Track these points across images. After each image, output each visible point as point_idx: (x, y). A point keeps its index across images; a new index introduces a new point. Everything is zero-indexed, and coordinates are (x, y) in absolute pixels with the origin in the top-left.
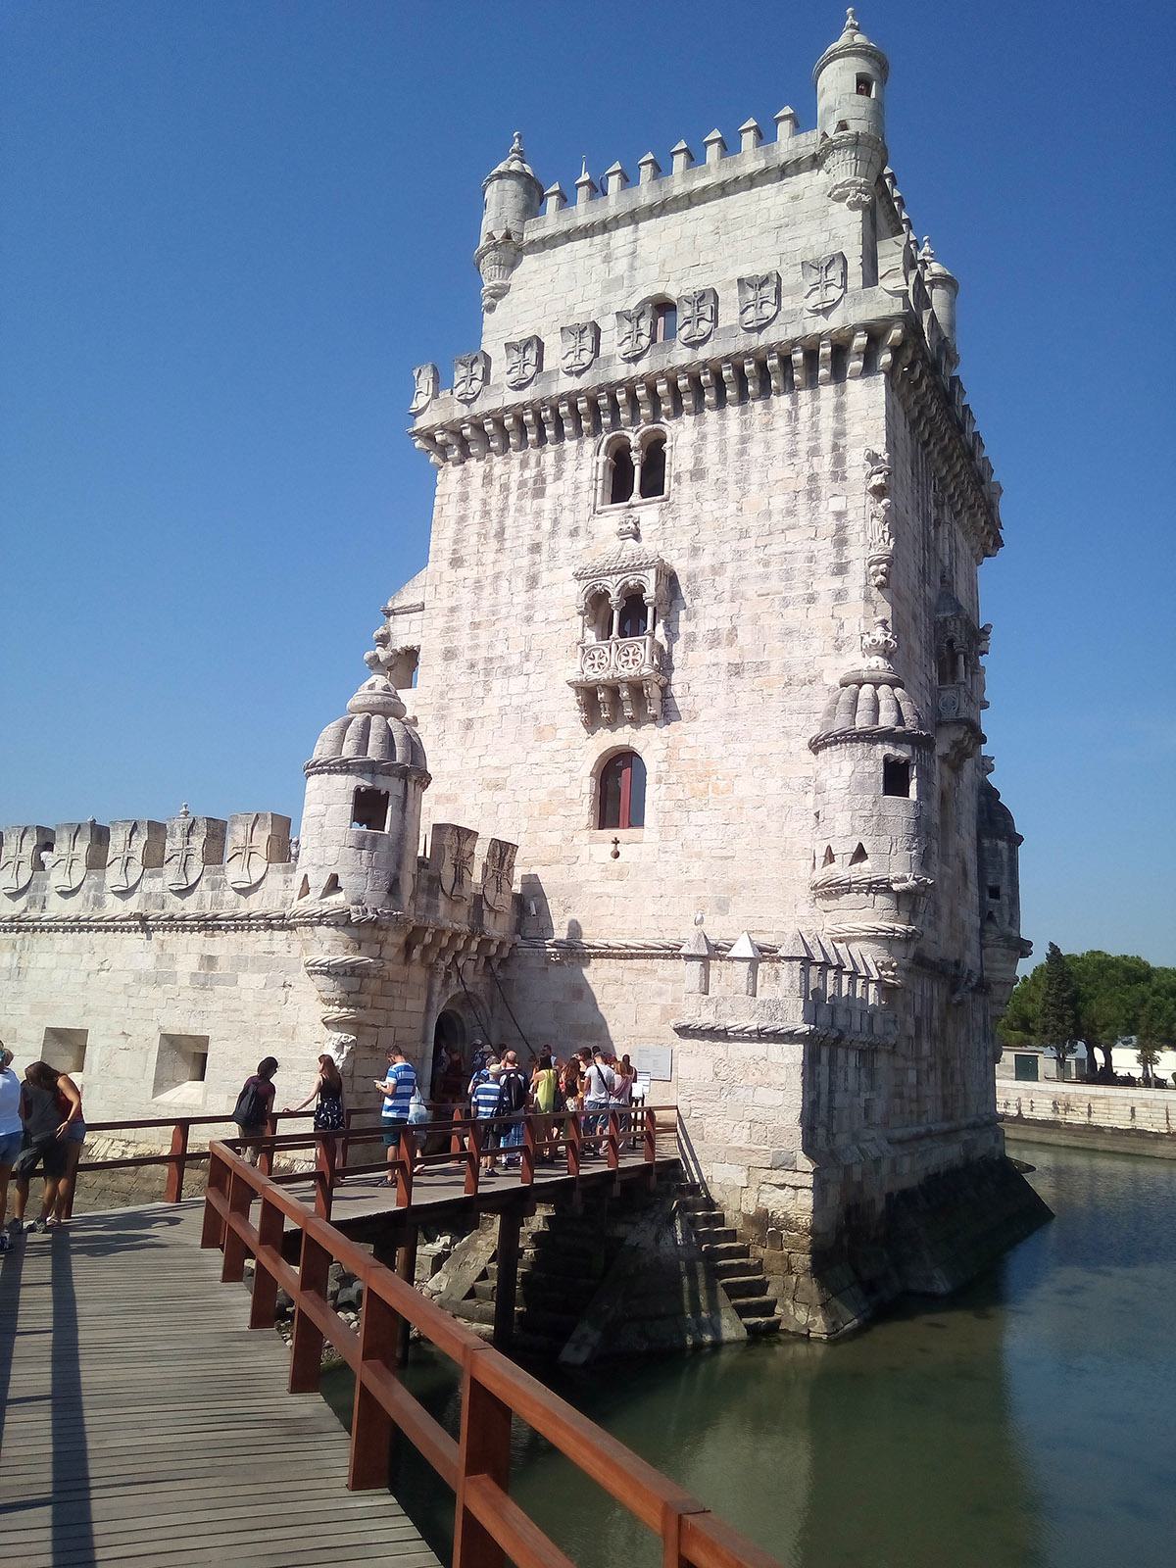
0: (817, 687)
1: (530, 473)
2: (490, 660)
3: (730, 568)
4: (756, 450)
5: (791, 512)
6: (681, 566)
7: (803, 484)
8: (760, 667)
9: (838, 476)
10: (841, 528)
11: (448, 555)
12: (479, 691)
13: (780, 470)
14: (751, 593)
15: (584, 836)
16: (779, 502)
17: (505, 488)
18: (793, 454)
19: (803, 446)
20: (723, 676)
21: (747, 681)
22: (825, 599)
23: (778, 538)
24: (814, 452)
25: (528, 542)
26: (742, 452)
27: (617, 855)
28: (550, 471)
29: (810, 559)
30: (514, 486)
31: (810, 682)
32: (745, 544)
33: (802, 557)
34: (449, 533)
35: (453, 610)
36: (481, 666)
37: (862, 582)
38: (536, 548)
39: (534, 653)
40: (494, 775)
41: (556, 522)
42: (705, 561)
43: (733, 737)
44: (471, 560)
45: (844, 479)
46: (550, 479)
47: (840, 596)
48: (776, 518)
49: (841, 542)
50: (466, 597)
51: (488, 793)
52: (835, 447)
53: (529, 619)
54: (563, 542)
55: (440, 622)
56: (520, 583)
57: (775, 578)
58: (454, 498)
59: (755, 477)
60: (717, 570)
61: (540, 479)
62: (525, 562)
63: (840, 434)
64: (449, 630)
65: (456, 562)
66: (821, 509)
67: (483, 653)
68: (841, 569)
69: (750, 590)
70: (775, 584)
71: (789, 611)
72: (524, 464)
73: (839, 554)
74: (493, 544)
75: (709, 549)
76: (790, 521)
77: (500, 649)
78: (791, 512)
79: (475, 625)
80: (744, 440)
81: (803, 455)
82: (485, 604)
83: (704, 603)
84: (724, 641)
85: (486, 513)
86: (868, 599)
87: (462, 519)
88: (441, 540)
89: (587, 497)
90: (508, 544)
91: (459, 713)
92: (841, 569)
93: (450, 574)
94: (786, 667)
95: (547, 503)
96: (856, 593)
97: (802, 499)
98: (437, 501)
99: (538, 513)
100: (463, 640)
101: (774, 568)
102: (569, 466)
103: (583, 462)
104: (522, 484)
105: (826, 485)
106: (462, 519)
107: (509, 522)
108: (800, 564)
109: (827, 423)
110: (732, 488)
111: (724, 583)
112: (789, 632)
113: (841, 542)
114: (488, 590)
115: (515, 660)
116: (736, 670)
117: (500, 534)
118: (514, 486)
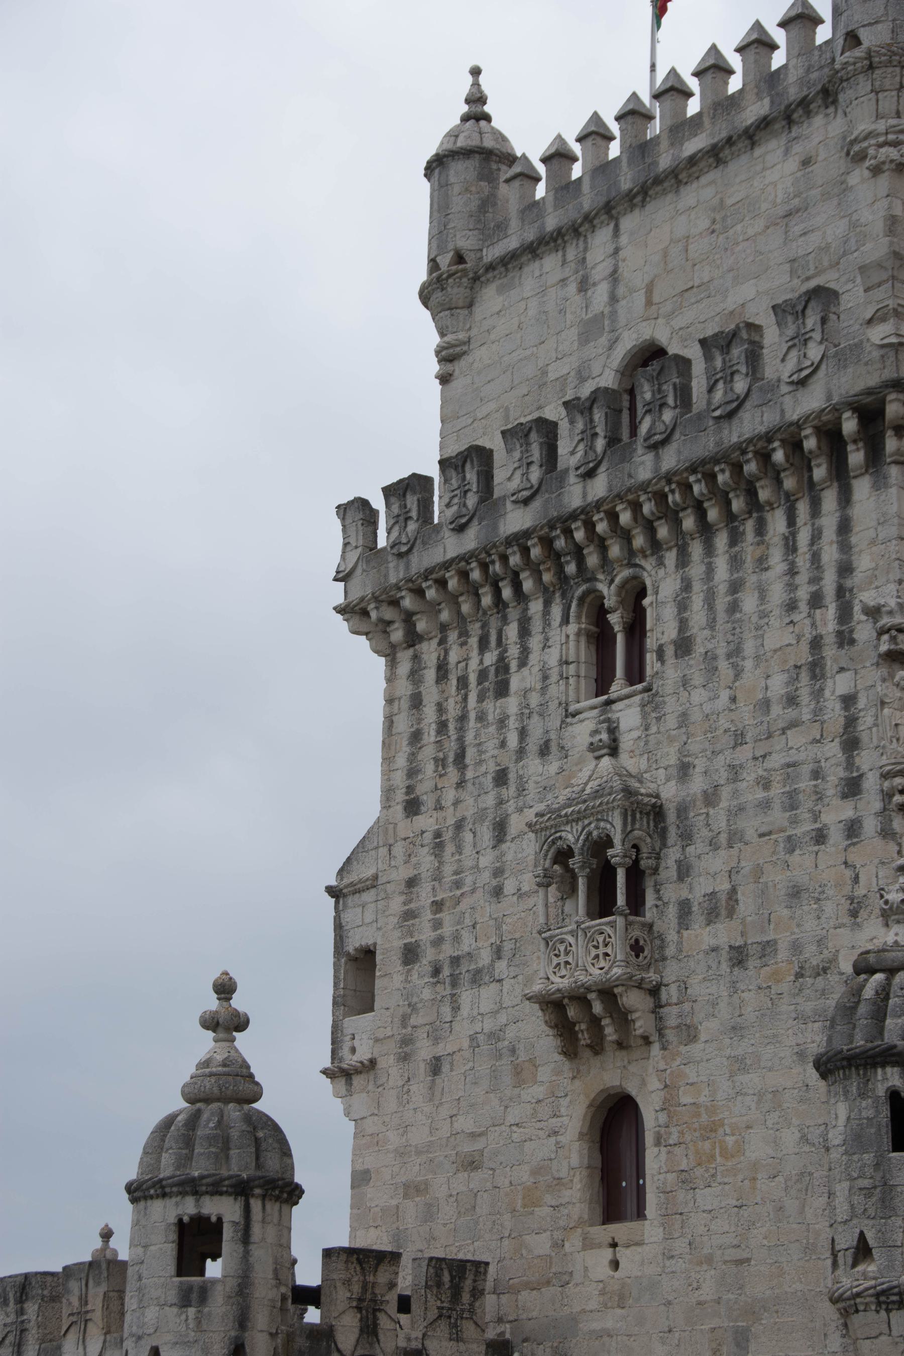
0: (833, 978)
1: (490, 658)
2: (455, 961)
3: (725, 792)
4: (749, 603)
7: (804, 655)
8: (768, 948)
9: (845, 639)
10: (851, 722)
12: (446, 1010)
13: (777, 635)
16: (778, 685)
17: (463, 682)
18: (791, 606)
19: (803, 594)
20: (725, 967)
22: (836, 836)
23: (778, 743)
24: (816, 601)
25: (492, 767)
26: (734, 608)
28: (514, 651)
29: (816, 774)
30: (473, 678)
31: (825, 970)
32: (744, 754)
33: (806, 770)
35: (412, 883)
36: (446, 972)
37: (878, 805)
38: (501, 778)
39: (508, 946)
40: (467, 1147)
42: (697, 784)
43: (739, 1065)
44: (428, 801)
45: (852, 642)
46: (514, 665)
47: (853, 829)
48: (776, 710)
49: (851, 744)
50: (426, 860)
52: (841, 592)
53: (498, 892)
54: (533, 766)
56: (486, 834)
57: (777, 806)
59: (749, 647)
60: (710, 798)
61: (502, 666)
62: (490, 800)
63: (845, 569)
64: (409, 915)
66: (827, 693)
67: (448, 950)
68: (852, 788)
69: (750, 825)
70: (778, 816)
71: (795, 858)
73: (850, 764)
75: (700, 764)
77: (467, 943)
78: (792, 700)
80: (735, 587)
81: (803, 606)
83: (699, 851)
84: (723, 912)
90: (469, 774)
91: (424, 1051)
94: (796, 947)
95: (512, 704)
96: (870, 825)
99: (502, 722)
100: (425, 934)
101: (777, 790)
102: (535, 642)
104: (483, 675)
105: (830, 652)
107: (470, 737)
108: (805, 784)
109: (830, 554)
110: (723, 665)
112: (795, 893)
113: (851, 744)
114: (450, 848)
115: (485, 958)
116: (739, 957)
117: (460, 756)
118: (473, 678)
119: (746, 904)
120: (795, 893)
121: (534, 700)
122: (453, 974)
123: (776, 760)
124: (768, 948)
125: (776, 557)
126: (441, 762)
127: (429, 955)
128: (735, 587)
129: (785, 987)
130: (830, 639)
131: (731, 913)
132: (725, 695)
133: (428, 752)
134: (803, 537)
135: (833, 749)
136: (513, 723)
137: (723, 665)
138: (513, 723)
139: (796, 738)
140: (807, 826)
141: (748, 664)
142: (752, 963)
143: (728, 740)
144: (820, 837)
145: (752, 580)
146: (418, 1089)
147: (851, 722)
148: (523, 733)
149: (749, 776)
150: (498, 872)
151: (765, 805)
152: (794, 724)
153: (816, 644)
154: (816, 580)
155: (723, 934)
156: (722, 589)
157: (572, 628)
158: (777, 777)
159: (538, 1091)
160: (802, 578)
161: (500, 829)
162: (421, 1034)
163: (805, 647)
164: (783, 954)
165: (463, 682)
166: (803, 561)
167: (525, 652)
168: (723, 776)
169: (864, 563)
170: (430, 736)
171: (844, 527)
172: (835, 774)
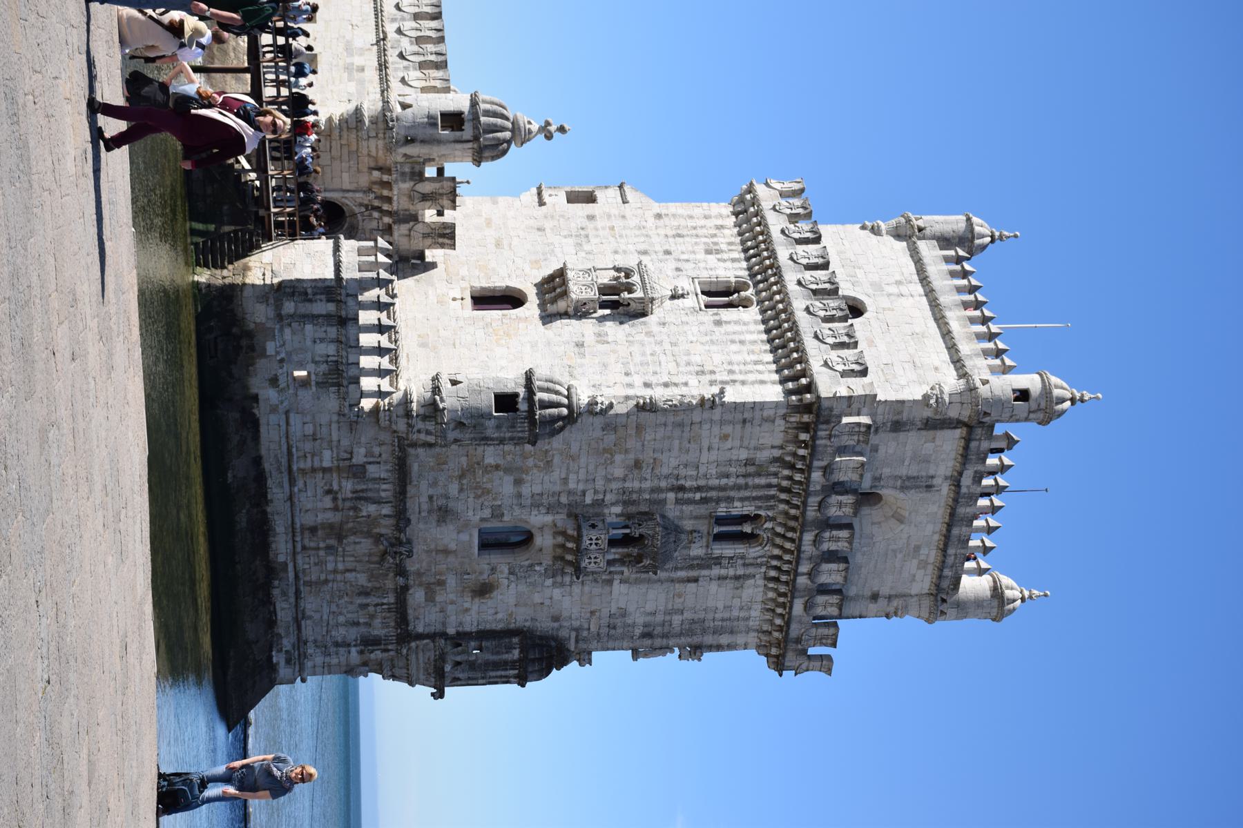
1: (724, 247)
2: (587, 236)
3: (651, 339)
4: (734, 347)
5: (688, 364)
6: (651, 319)
7: (707, 368)
8: (583, 355)
9: (712, 383)
10: (676, 385)
11: (664, 212)
12: (565, 233)
13: (718, 358)
14: (632, 349)
15: (466, 285)
16: (697, 359)
17: (715, 236)
18: (730, 363)
19: (735, 368)
21: (572, 349)
22: (628, 380)
23: (672, 358)
24: (731, 372)
25: (672, 249)
26: (733, 342)
27: (454, 299)
28: (725, 256)
30: (715, 240)
32: (667, 346)
34: (680, 211)
35: (624, 217)
36: (582, 232)
38: (668, 252)
39: (591, 257)
40: (505, 242)
41: (688, 261)
42: (655, 329)
43: (534, 345)
44: (660, 223)
46: (719, 256)
47: (630, 385)
48: (685, 358)
49: (666, 385)
50: (633, 222)
51: (493, 241)
52: (734, 381)
53: (616, 252)
54: (673, 265)
55: (614, 211)
56: (642, 247)
58: (707, 213)
59: (714, 348)
60: (649, 334)
61: (718, 252)
62: (658, 248)
63: (743, 383)
64: (609, 216)
65: (659, 216)
67: (591, 233)
68: (647, 385)
69: (635, 349)
70: (638, 359)
71: (620, 365)
72: (730, 244)
73: (658, 385)
74: (670, 233)
75: (665, 330)
76: (683, 363)
77: (593, 240)
79: (612, 228)
80: (742, 342)
81: (730, 367)
82: (628, 232)
85: (695, 228)
86: (627, 398)
87: (691, 217)
88: (673, 208)
89: (705, 275)
90: (671, 240)
91: (548, 225)
92: (647, 385)
93: (649, 215)
94: (581, 366)
95: (701, 256)
96: (631, 392)
97: (699, 369)
98: (705, 205)
99: (694, 252)
100: (599, 223)
101: (650, 358)
102: (729, 264)
103: (732, 269)
104: (716, 244)
105: (708, 377)
106: (691, 217)
107: (687, 239)
109: (751, 377)
110: (708, 338)
111: (642, 337)
112: (605, 366)
113: (666, 385)
114: (637, 232)
115: (587, 247)
117: (679, 236)
118: (715, 240)
120: (605, 366)
121: (702, 265)
122: (582, 236)
123: (663, 358)
124: (583, 355)
126: (678, 227)
127: (590, 225)
128: (742, 342)
130: (713, 377)
131: (598, 342)
132: (694, 339)
133: (683, 222)
134: (760, 367)
135: (665, 379)
136: (692, 257)
137: (708, 338)
138: (692, 257)
139: (672, 367)
140: (632, 369)
141: (707, 348)
142: (576, 349)
144: (627, 374)
145: (744, 348)
146: (532, 222)
147: (676, 385)
148: (688, 261)
149: (658, 349)
150: (625, 252)
151: (644, 354)
153: (713, 372)
154: (741, 372)
155: (589, 339)
156: (742, 338)
157: (733, 280)
158: (655, 358)
159: (527, 270)
160: (742, 367)
161: (645, 253)
162: (556, 223)
163: (711, 368)
164: (579, 361)
165: (715, 236)
166: (750, 367)
167: (725, 261)
168: (659, 339)
169: (746, 389)
170: (690, 223)
171: (762, 382)
172: (653, 380)
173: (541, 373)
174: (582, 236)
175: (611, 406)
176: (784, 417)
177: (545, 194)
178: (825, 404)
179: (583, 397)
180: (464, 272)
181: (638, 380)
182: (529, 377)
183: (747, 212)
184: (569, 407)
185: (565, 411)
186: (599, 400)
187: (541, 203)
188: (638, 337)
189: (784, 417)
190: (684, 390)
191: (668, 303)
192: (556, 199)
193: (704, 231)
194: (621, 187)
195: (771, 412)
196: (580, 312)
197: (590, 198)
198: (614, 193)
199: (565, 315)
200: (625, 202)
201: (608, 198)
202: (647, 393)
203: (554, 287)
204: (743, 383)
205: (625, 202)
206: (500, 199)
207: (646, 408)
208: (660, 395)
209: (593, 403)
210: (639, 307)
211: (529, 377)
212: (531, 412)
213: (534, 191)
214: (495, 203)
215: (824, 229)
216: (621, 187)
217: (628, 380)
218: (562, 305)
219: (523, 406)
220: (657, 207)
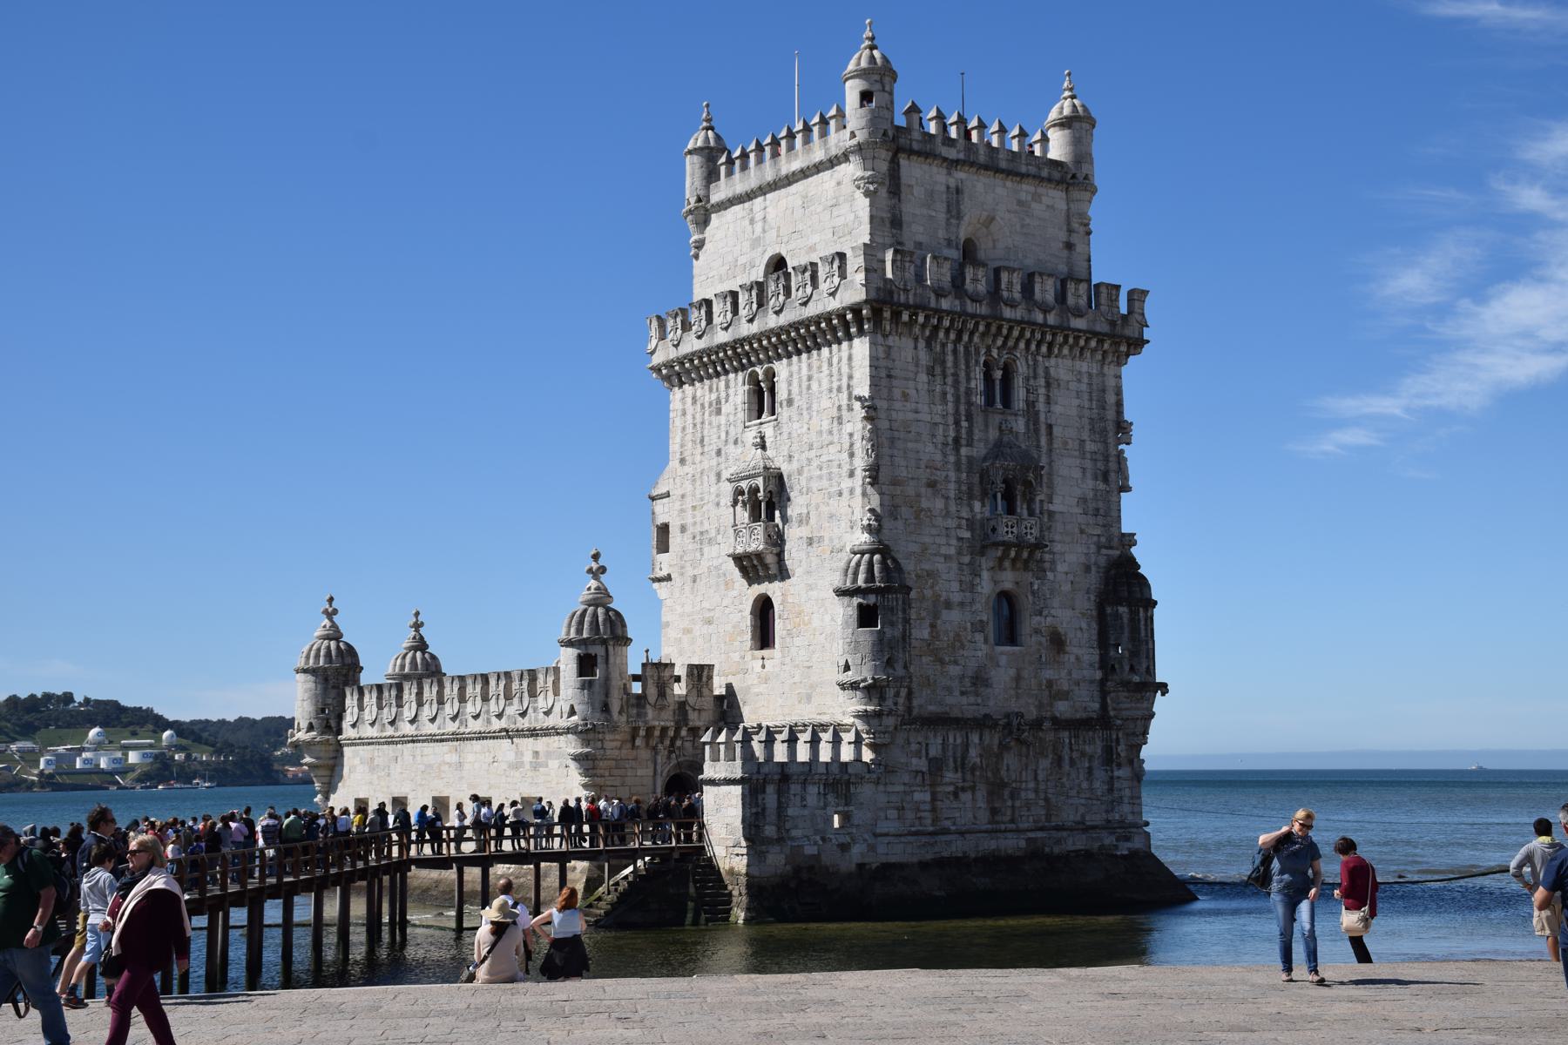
1: (714, 396)
4: (815, 386)
5: (831, 432)
7: (835, 413)
8: (821, 539)
9: (850, 409)
10: (852, 445)
13: (826, 403)
16: (826, 425)
17: (702, 405)
18: (830, 391)
19: (835, 385)
21: (815, 550)
22: (846, 494)
23: (825, 450)
24: (839, 389)
26: (809, 388)
28: (723, 395)
29: (839, 466)
32: (812, 454)
34: (678, 440)
35: (683, 496)
38: (719, 453)
42: (795, 465)
43: (810, 587)
47: (852, 491)
49: (852, 455)
50: (688, 487)
52: (849, 386)
53: (718, 504)
54: (731, 447)
55: (677, 505)
56: (713, 478)
59: (815, 407)
60: (800, 472)
61: (718, 402)
62: (714, 462)
63: (850, 377)
64: (682, 511)
65: (683, 461)
67: (699, 528)
68: (852, 474)
69: (815, 485)
70: (825, 483)
72: (711, 390)
74: (699, 450)
75: (796, 456)
77: (706, 526)
79: (694, 508)
80: (810, 378)
86: (864, 494)
87: (684, 429)
88: (674, 447)
89: (741, 415)
91: (690, 572)
92: (852, 474)
93: (681, 470)
94: (831, 540)
95: (722, 419)
96: (858, 491)
100: (689, 521)
101: (825, 471)
102: (731, 391)
103: (736, 389)
104: (711, 404)
106: (684, 429)
108: (835, 470)
109: (845, 369)
112: (831, 516)
113: (852, 455)
115: (713, 533)
116: (810, 541)
117: (702, 441)
119: (813, 521)
120: (831, 516)
121: (732, 418)
122: (702, 539)
123: (824, 458)
124: (821, 539)
125: (825, 366)
127: (690, 530)
128: (810, 378)
129: (827, 555)
130: (844, 407)
133: (689, 437)
134: (835, 360)
135: (845, 456)
136: (723, 428)
138: (723, 428)
139: (833, 449)
140: (835, 489)
143: (806, 447)
144: (840, 494)
146: (687, 588)
147: (852, 445)
149: (815, 463)
151: (820, 477)
152: (831, 443)
153: (839, 408)
159: (735, 593)
161: (719, 475)
165: (702, 405)
166: (835, 371)
169: (857, 375)
170: (690, 430)
171: (850, 358)
172: (846, 468)
173: (837, 580)
174: (702, 539)
175: (872, 511)
176: (885, 336)
177: (660, 574)
178: (873, 295)
179: (864, 538)
180: (736, 657)
181: (846, 484)
182: (841, 593)
183: (679, 373)
184: (872, 552)
185: (877, 557)
186: (865, 522)
187: (668, 578)
188: (803, 483)
189: (885, 336)
190: (858, 437)
191: (769, 453)
192: (665, 563)
193: (698, 416)
194: (653, 499)
195: (881, 349)
196: (777, 541)
197: (664, 530)
198: (659, 506)
199: (780, 556)
200: (668, 495)
201: (664, 512)
202: (859, 474)
203: (752, 567)
204: (850, 377)
205: (668, 495)
206: (664, 619)
207: (875, 475)
208: (861, 462)
209: (869, 529)
210: (773, 481)
211: (841, 593)
212: (877, 591)
213: (656, 585)
214: (667, 624)
215: (698, 296)
216: (653, 499)
217: (846, 494)
218: (770, 559)
219: (872, 599)
220: (674, 463)
